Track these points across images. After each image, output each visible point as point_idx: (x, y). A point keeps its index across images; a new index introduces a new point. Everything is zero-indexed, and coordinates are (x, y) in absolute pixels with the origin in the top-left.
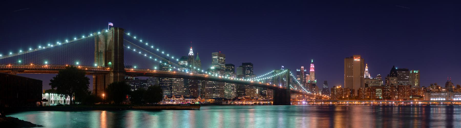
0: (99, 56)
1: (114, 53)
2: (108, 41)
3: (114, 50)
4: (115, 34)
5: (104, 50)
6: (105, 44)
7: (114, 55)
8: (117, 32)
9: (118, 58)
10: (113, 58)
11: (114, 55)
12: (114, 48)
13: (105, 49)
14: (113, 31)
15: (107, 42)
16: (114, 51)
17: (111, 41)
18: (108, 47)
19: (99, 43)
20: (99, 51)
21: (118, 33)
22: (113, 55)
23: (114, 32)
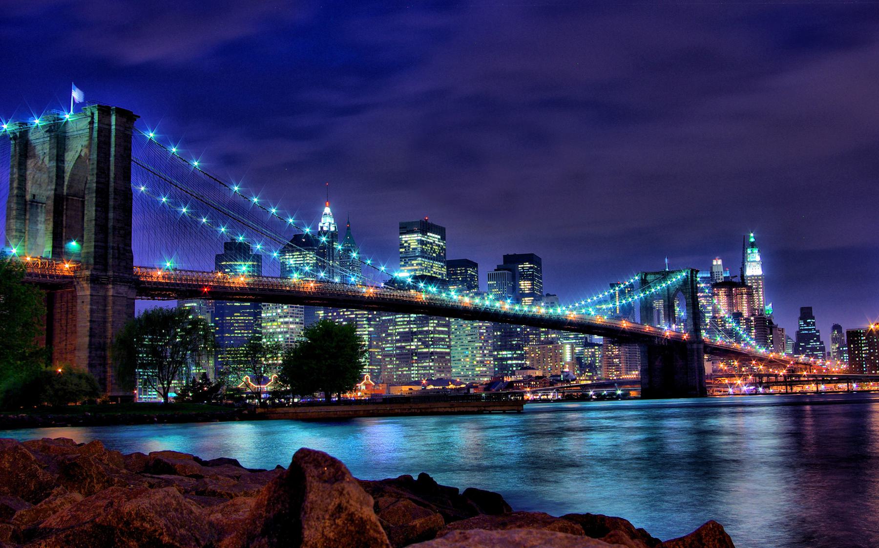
0: (27, 217)
1: (97, 205)
2: (70, 158)
3: (94, 195)
4: (100, 131)
5: (53, 192)
6: (55, 169)
7: (96, 215)
8: (110, 125)
9: (111, 224)
10: (89, 227)
11: (94, 213)
12: (95, 185)
13: (56, 190)
14: (93, 118)
15: (63, 161)
16: (96, 197)
17: (80, 156)
18: (66, 183)
19: (30, 163)
20: (28, 197)
21: (113, 127)
22: (90, 212)
23: (96, 125)
